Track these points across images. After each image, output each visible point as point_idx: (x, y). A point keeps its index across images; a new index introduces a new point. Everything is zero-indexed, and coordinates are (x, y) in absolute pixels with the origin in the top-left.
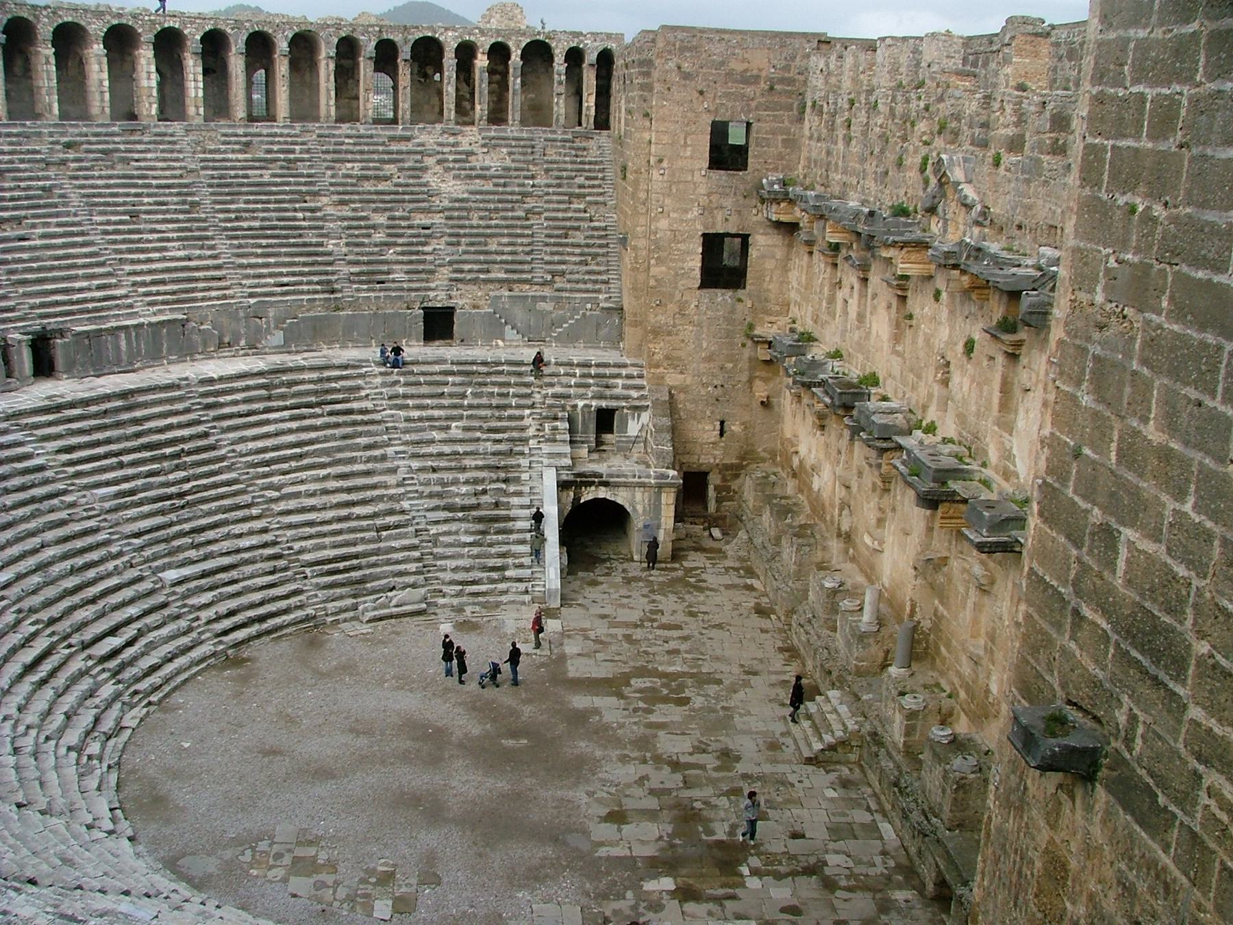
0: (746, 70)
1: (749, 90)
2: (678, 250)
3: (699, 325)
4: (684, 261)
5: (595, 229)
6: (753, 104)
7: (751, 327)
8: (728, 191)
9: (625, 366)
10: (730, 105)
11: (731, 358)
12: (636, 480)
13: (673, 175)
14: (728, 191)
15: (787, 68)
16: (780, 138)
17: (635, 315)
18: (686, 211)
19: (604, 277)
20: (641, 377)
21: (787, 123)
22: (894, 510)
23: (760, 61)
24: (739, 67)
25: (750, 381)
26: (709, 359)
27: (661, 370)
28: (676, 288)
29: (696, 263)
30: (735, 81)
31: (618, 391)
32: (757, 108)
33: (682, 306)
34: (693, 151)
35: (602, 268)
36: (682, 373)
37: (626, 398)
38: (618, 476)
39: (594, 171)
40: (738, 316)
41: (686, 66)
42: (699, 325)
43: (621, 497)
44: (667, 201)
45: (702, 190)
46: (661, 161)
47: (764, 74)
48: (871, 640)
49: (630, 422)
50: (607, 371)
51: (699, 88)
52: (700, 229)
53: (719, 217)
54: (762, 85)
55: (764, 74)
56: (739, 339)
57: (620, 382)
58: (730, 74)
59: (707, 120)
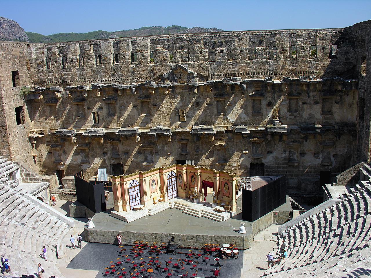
1: (17, 61)
4: (12, 118)
6: (18, 65)
7: (28, 135)
12: (42, 188)
15: (23, 53)
18: (10, 102)
21: (25, 70)
26: (22, 148)
27: (14, 156)
29: (15, 118)
36: (18, 155)
38: (39, 189)
42: (18, 138)
43: (41, 195)
45: (13, 94)
49: (16, 174)
52: (15, 107)
53: (17, 102)
54: (19, 59)
56: (27, 140)
59: (11, 71)
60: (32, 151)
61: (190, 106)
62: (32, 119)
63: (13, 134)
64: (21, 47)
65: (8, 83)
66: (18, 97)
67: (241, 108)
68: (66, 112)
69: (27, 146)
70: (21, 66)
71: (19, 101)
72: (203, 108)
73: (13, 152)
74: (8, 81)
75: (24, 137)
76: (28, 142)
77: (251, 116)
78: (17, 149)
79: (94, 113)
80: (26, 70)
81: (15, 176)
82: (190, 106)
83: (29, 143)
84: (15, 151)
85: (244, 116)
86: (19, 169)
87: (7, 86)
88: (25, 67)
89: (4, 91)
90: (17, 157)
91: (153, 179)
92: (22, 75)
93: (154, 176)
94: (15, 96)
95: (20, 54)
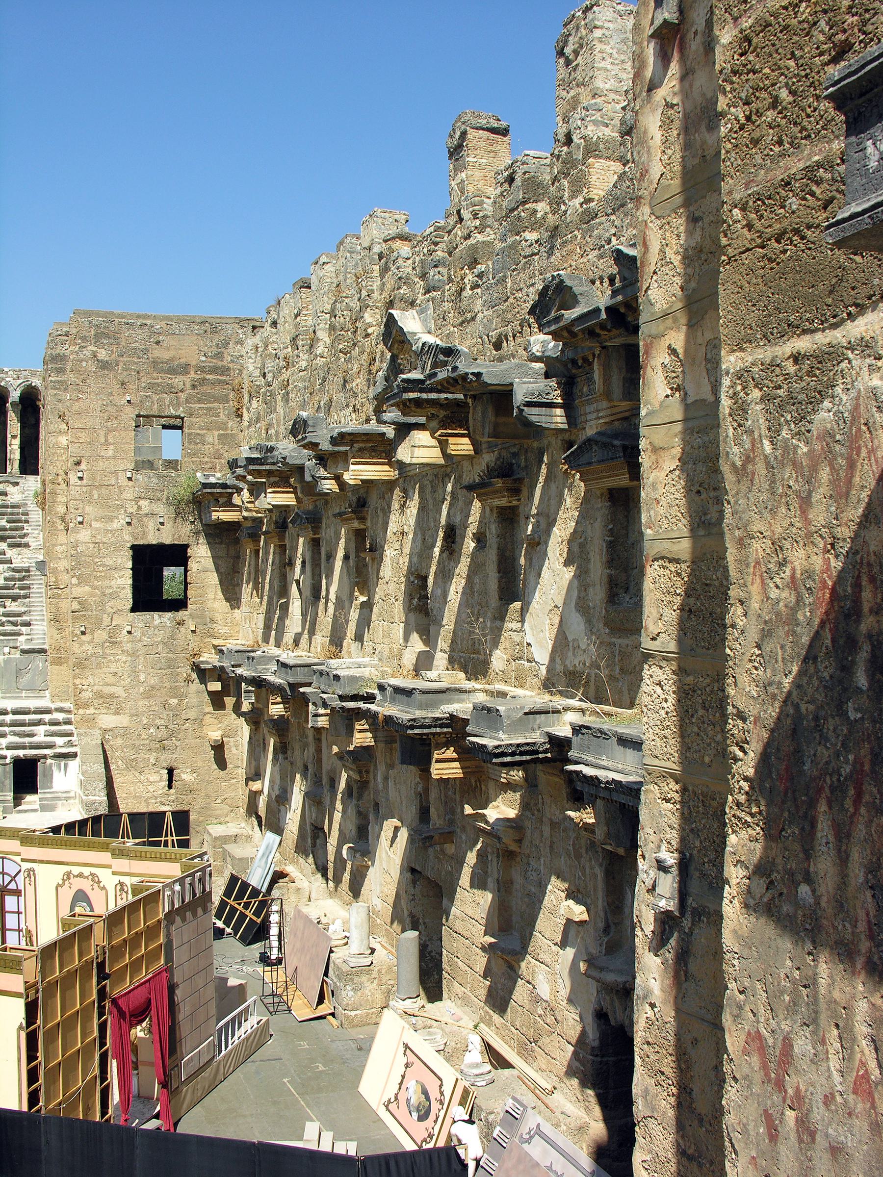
0: (172, 359)
1: (177, 381)
2: (104, 565)
3: (134, 654)
5: (14, 570)
6: (183, 396)
8: (158, 495)
9: (48, 711)
10: (155, 397)
11: (174, 692)
13: (94, 479)
14: (158, 495)
15: (219, 356)
16: (216, 433)
17: (58, 650)
18: (111, 519)
19: (25, 618)
20: (68, 722)
22: (377, 806)
23: (191, 350)
24: (166, 355)
25: (199, 722)
26: (148, 695)
27: (91, 710)
28: (103, 611)
30: (162, 371)
31: (40, 738)
32: (187, 401)
33: (113, 632)
34: (116, 450)
35: (23, 609)
37: (50, 746)
39: (18, 514)
40: (180, 641)
41: (102, 354)
42: (134, 654)
44: (88, 509)
45: (129, 495)
46: (78, 463)
47: (193, 363)
48: (364, 978)
50: (27, 718)
51: (120, 378)
52: (128, 540)
53: (151, 525)
54: (193, 375)
55: (193, 363)
56: (185, 670)
57: (41, 730)
58: (155, 362)
60: (208, 719)
61: (437, 551)
62: (233, 597)
63: (101, 635)
64: (216, 337)
65: (110, 453)
66: (160, 509)
67: (567, 563)
68: (268, 578)
69: (181, 697)
70: (199, 401)
71: (162, 524)
72: (463, 567)
73: (86, 695)
74: (112, 447)
75: (169, 660)
76: (188, 680)
77: (601, 625)
78: (119, 691)
79: (298, 582)
80: (228, 416)
81: (49, 776)
82: (437, 551)
83: (196, 686)
84: (99, 695)
85: (577, 626)
86: (75, 755)
87: (101, 465)
88: (223, 413)
89: (81, 478)
90: (108, 720)
91: (79, 884)
92: (203, 435)
93: (86, 871)
94: (144, 503)
95: (204, 359)
